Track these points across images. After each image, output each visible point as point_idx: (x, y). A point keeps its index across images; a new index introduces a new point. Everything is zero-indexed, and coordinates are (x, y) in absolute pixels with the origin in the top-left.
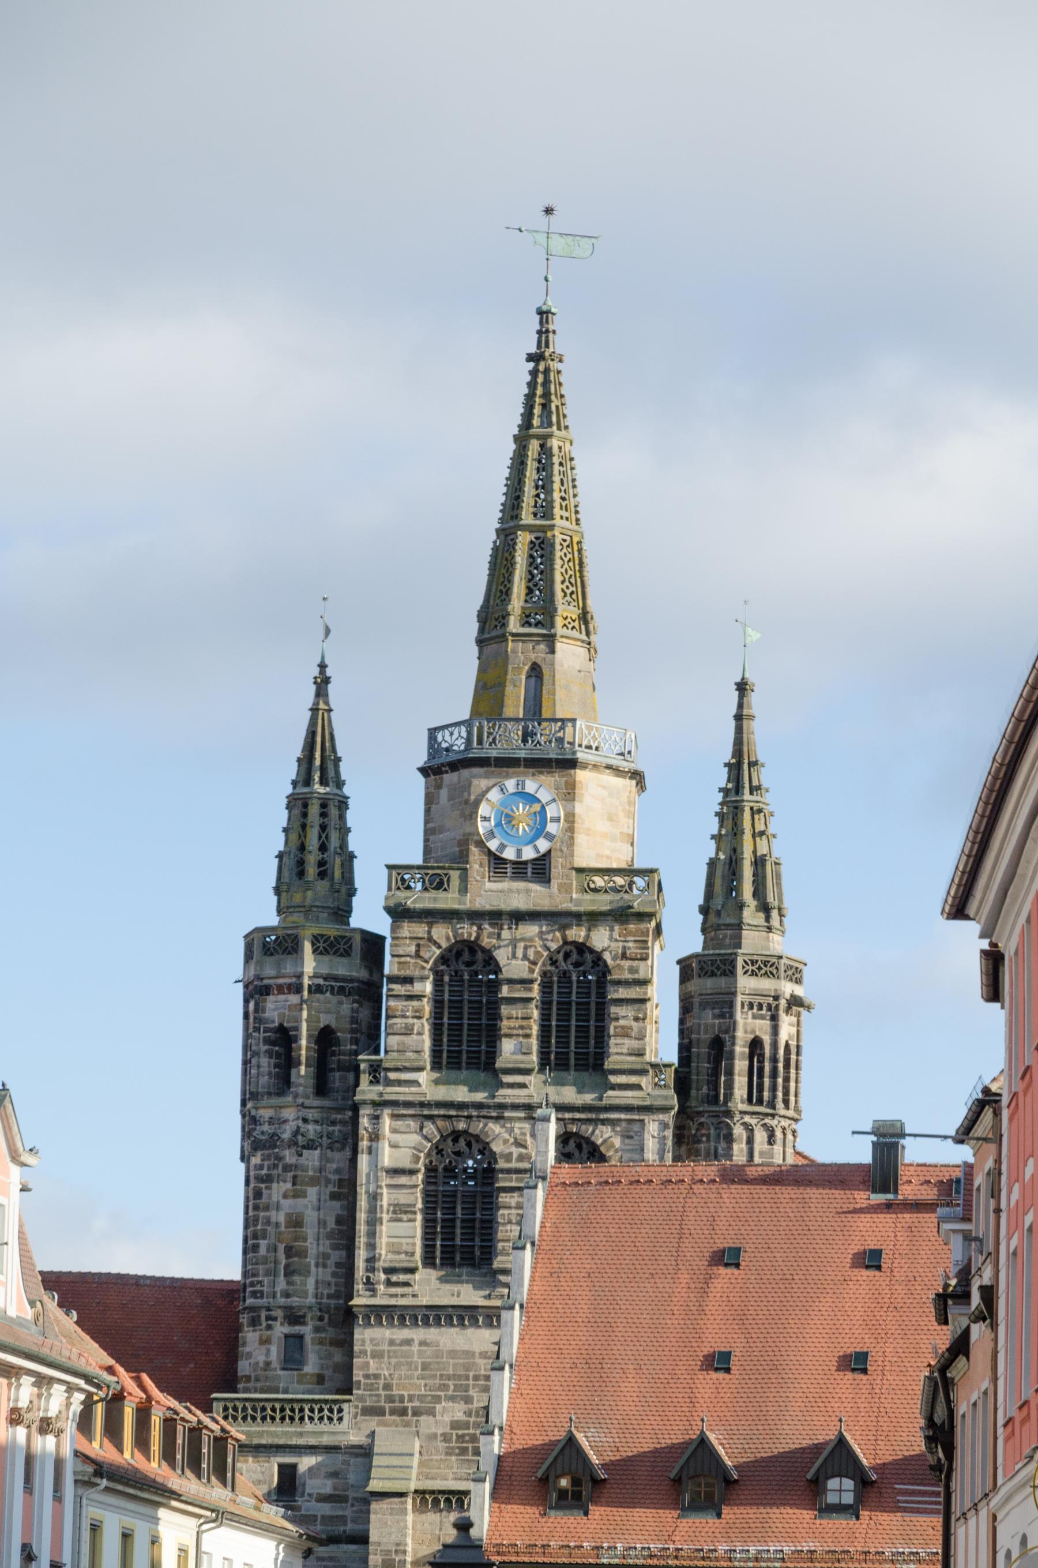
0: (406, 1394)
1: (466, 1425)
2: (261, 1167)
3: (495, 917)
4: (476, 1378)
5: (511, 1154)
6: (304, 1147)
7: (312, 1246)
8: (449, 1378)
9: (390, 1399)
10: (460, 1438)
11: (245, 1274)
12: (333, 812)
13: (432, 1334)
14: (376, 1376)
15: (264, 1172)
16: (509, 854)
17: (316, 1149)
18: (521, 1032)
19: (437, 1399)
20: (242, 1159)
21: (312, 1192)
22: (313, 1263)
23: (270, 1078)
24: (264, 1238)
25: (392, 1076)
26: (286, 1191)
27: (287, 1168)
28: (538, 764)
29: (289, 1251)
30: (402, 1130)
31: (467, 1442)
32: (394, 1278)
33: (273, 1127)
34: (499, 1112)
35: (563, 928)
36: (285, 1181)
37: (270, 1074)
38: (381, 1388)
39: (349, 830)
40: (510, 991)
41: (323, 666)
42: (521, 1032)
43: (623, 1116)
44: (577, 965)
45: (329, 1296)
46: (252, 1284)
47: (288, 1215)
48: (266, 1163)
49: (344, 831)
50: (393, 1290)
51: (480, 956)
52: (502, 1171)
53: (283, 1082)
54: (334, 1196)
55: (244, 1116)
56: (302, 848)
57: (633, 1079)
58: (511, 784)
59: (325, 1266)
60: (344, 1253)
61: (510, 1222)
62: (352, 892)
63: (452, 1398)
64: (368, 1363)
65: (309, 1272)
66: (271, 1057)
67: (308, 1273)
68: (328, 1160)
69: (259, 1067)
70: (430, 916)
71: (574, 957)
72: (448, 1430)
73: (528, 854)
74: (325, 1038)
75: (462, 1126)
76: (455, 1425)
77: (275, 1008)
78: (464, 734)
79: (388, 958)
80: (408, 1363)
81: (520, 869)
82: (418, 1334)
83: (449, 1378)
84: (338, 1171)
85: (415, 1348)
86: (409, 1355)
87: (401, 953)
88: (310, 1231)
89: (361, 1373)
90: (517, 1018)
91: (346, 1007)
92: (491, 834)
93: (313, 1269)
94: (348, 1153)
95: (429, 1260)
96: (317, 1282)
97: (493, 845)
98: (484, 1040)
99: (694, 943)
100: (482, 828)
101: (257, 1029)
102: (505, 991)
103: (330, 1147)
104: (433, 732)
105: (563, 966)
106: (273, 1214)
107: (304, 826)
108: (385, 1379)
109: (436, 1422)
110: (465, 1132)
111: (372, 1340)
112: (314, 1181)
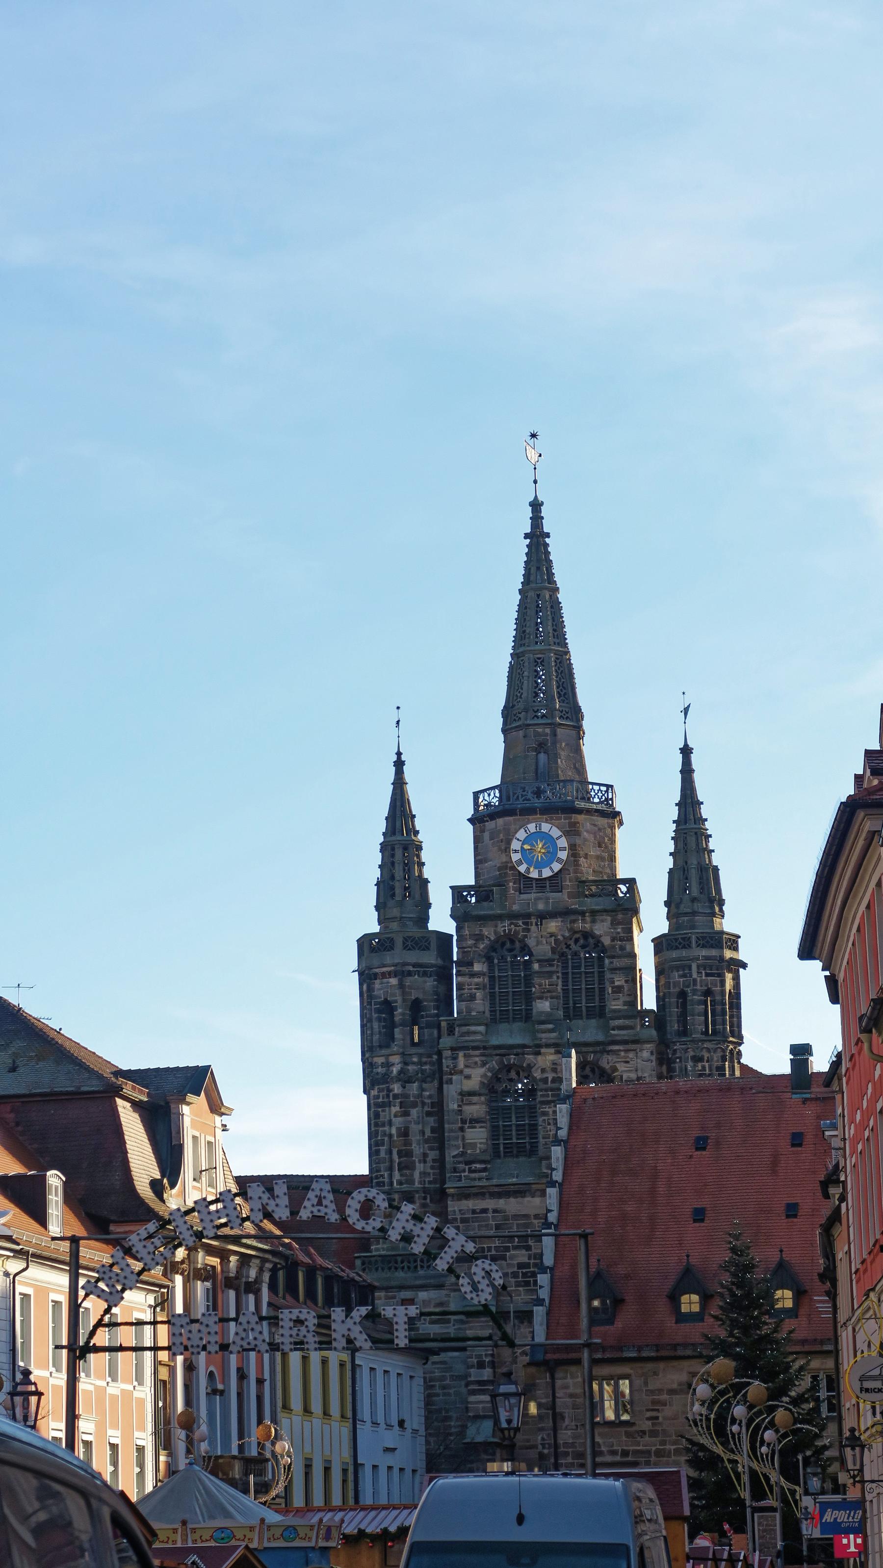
0: (485, 1246)
2: (378, 1097)
7: (417, 1149)
10: (524, 1275)
11: (371, 1170)
13: (501, 1203)
15: (380, 1100)
16: (534, 874)
17: (414, 1082)
18: (549, 994)
19: (507, 1249)
20: (365, 1092)
21: (414, 1112)
22: (417, 1160)
24: (383, 1145)
25: (465, 1029)
27: (396, 1096)
28: (549, 811)
29: (400, 1153)
32: (474, 1166)
36: (395, 1106)
40: (540, 966)
41: (399, 754)
43: (621, 1048)
45: (430, 1182)
46: (377, 1177)
47: (398, 1129)
48: (381, 1094)
50: (473, 1175)
51: (518, 945)
53: (389, 1038)
54: (429, 1114)
56: (393, 877)
57: (627, 1022)
58: (532, 827)
59: (425, 1162)
60: (437, 1152)
62: (429, 906)
63: (516, 1248)
65: (415, 1166)
68: (423, 1090)
69: (372, 1028)
71: (582, 941)
72: (515, 1269)
73: (547, 873)
74: (416, 1006)
76: (521, 1266)
78: (498, 795)
79: (455, 949)
81: (541, 883)
82: (490, 1204)
84: (430, 1097)
86: (487, 1219)
88: (415, 1138)
92: (520, 863)
93: (417, 1164)
94: (436, 1083)
95: (497, 1155)
96: (420, 1173)
97: (522, 869)
99: (663, 927)
100: (515, 857)
101: (370, 1003)
102: (536, 966)
104: (476, 795)
105: (574, 947)
106: (386, 1128)
107: (393, 864)
109: (508, 1265)
111: (460, 1211)
112: (414, 1105)
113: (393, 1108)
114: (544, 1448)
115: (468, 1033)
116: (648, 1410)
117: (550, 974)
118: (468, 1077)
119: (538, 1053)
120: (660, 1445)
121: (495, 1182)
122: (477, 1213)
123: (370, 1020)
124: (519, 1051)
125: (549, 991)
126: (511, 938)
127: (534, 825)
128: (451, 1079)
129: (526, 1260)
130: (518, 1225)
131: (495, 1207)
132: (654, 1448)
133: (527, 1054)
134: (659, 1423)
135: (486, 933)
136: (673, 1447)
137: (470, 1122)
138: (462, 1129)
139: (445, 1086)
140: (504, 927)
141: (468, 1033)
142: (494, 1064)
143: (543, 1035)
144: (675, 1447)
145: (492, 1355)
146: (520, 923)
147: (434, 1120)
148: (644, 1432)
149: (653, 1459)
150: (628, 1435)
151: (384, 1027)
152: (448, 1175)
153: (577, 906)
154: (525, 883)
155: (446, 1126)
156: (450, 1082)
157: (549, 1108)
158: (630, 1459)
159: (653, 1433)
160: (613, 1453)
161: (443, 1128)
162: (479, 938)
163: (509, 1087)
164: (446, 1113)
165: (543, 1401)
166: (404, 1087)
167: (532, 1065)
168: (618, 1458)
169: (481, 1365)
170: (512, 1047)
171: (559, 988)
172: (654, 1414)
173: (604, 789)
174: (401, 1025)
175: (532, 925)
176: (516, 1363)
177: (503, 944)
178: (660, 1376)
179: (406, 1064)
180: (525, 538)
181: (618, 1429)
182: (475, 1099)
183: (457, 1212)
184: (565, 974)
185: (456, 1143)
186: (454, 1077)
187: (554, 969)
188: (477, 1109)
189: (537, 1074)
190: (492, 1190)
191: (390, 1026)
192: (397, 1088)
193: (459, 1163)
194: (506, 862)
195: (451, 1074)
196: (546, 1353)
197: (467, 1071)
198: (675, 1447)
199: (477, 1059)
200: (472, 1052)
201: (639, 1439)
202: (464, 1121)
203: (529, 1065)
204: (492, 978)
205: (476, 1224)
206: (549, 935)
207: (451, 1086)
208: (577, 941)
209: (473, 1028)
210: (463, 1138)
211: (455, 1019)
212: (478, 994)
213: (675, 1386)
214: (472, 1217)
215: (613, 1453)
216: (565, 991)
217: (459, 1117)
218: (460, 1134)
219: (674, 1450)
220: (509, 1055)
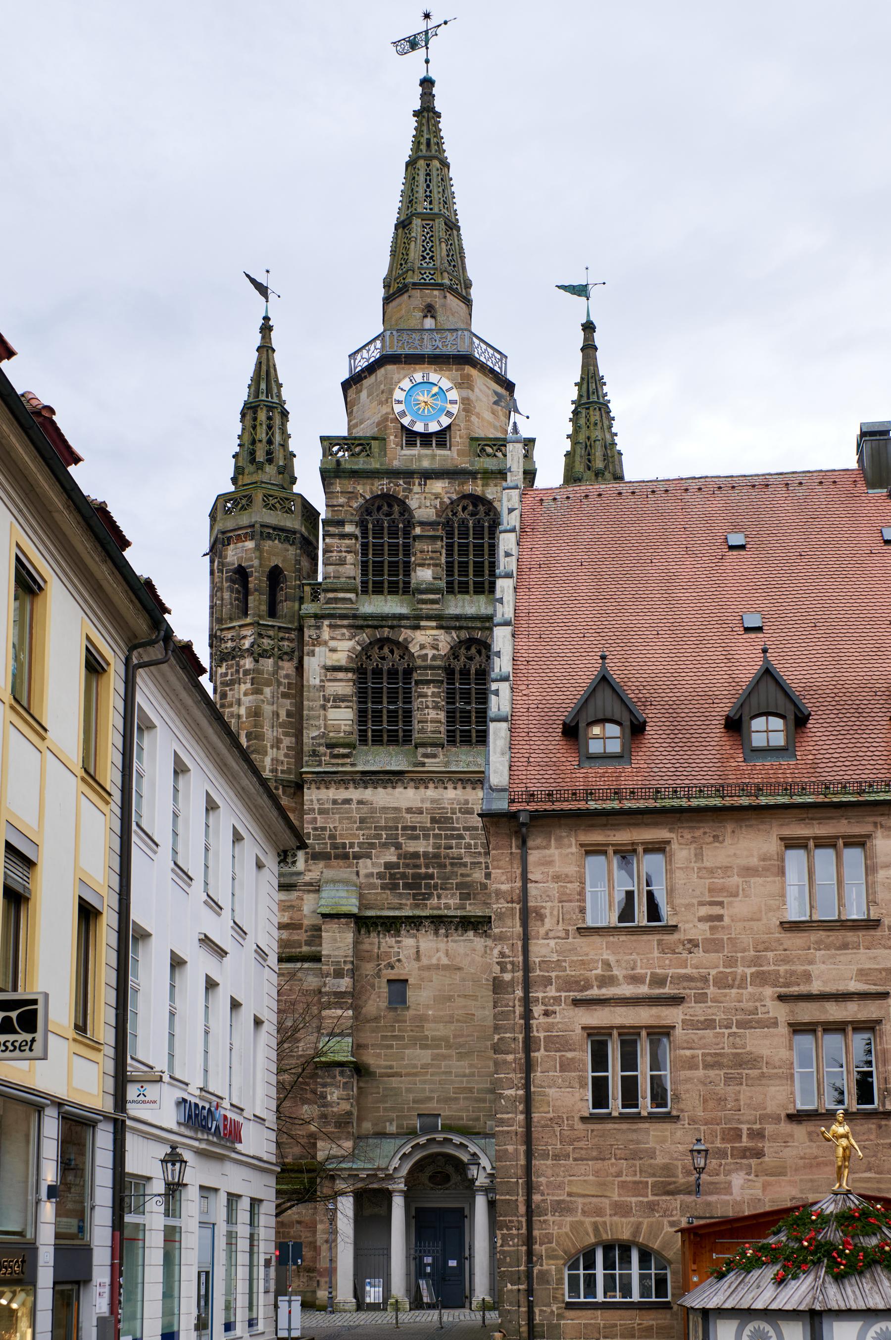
0: (347, 842)
1: (396, 865)
2: (226, 674)
3: (408, 474)
4: (404, 828)
5: (427, 655)
6: (260, 655)
8: (382, 828)
9: (335, 846)
12: (277, 420)
13: (368, 794)
14: (324, 829)
15: (229, 677)
17: (269, 658)
18: (432, 562)
19: (372, 846)
22: (269, 745)
23: (232, 607)
25: (331, 595)
26: (246, 690)
27: (246, 672)
28: (438, 360)
30: (339, 637)
31: (398, 879)
32: (336, 751)
33: (235, 643)
34: (415, 621)
35: (463, 484)
36: (245, 683)
37: (231, 604)
38: (327, 836)
39: (289, 436)
42: (432, 562)
44: (473, 514)
47: (248, 709)
48: (229, 671)
49: (286, 436)
51: (396, 508)
52: (420, 668)
55: (211, 646)
59: (278, 748)
61: (427, 707)
62: (293, 480)
64: (316, 818)
65: (266, 752)
66: (232, 592)
67: (265, 753)
69: (222, 599)
70: (355, 474)
71: (471, 508)
72: (382, 870)
75: (386, 632)
76: (388, 866)
77: (233, 555)
80: (348, 818)
81: (426, 439)
82: (354, 794)
83: (382, 828)
85: (354, 806)
87: (335, 503)
89: (311, 826)
90: (428, 552)
91: (292, 552)
93: (269, 750)
95: (363, 740)
96: (272, 760)
98: (401, 572)
102: (418, 531)
103: (281, 658)
105: (461, 515)
106: (235, 709)
108: (330, 830)
109: (373, 864)
110: (388, 640)
111: (318, 800)
112: (268, 685)
113: (242, 686)
114: (503, 970)
115: (336, 600)
116: (702, 904)
117: (434, 538)
118: (334, 650)
119: (417, 627)
120: (725, 967)
121: (359, 768)
122: (339, 804)
123: (221, 589)
124: (395, 623)
125: (431, 558)
126: (388, 499)
127: (421, 374)
128: (313, 651)
129: (394, 859)
130: (386, 818)
131: (360, 797)
132: (713, 972)
133: (406, 627)
134: (723, 928)
135: (361, 491)
136: (749, 971)
137: (334, 701)
138: (324, 707)
139: (306, 658)
140: (382, 486)
141: (336, 600)
142: (364, 637)
143: (424, 606)
144: (753, 969)
145: (352, 962)
146: (401, 482)
147: (291, 703)
148: (694, 943)
149: (712, 991)
150: (663, 949)
151: (237, 599)
152: (305, 759)
153: (468, 465)
154: (411, 437)
155: (305, 703)
156: (312, 653)
157: (428, 688)
158: (667, 990)
159: (714, 945)
160: (635, 979)
161: (301, 716)
162: (352, 495)
163: (380, 666)
164: (305, 689)
165: (504, 887)
166: (257, 661)
167: (409, 640)
168: (644, 990)
169: (339, 974)
170: (384, 617)
171: (443, 560)
172: (716, 910)
173: (498, 356)
174: (256, 590)
175: (414, 485)
176: (379, 977)
177: (379, 508)
178: (726, 843)
179: (260, 635)
180: (414, 115)
181: (645, 937)
182: (341, 675)
183: (315, 802)
184: (450, 547)
185: (317, 723)
186: (317, 649)
187: (439, 533)
188: (343, 686)
189: (414, 649)
190: (358, 777)
191: (246, 592)
192: (248, 663)
193: (320, 745)
194: (386, 414)
195: (314, 645)
196: (512, 801)
197: (332, 644)
198: (753, 969)
199: (345, 631)
200: (339, 622)
201: (685, 954)
202: (327, 700)
203: (406, 639)
204: (365, 546)
205: (337, 816)
206: (433, 497)
207: (312, 659)
208: (464, 509)
209: (341, 595)
210: (325, 719)
211: (320, 584)
212: (348, 557)
213: (754, 861)
214: (333, 809)
215: (635, 979)
216: (450, 565)
217: (322, 694)
218: (322, 712)
219: (752, 974)
220: (382, 627)
